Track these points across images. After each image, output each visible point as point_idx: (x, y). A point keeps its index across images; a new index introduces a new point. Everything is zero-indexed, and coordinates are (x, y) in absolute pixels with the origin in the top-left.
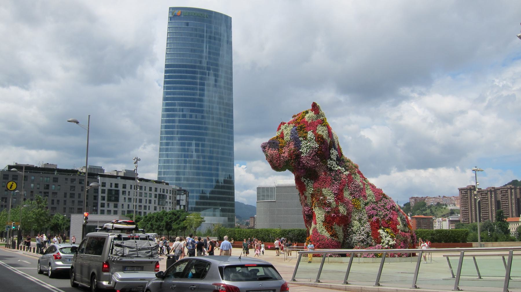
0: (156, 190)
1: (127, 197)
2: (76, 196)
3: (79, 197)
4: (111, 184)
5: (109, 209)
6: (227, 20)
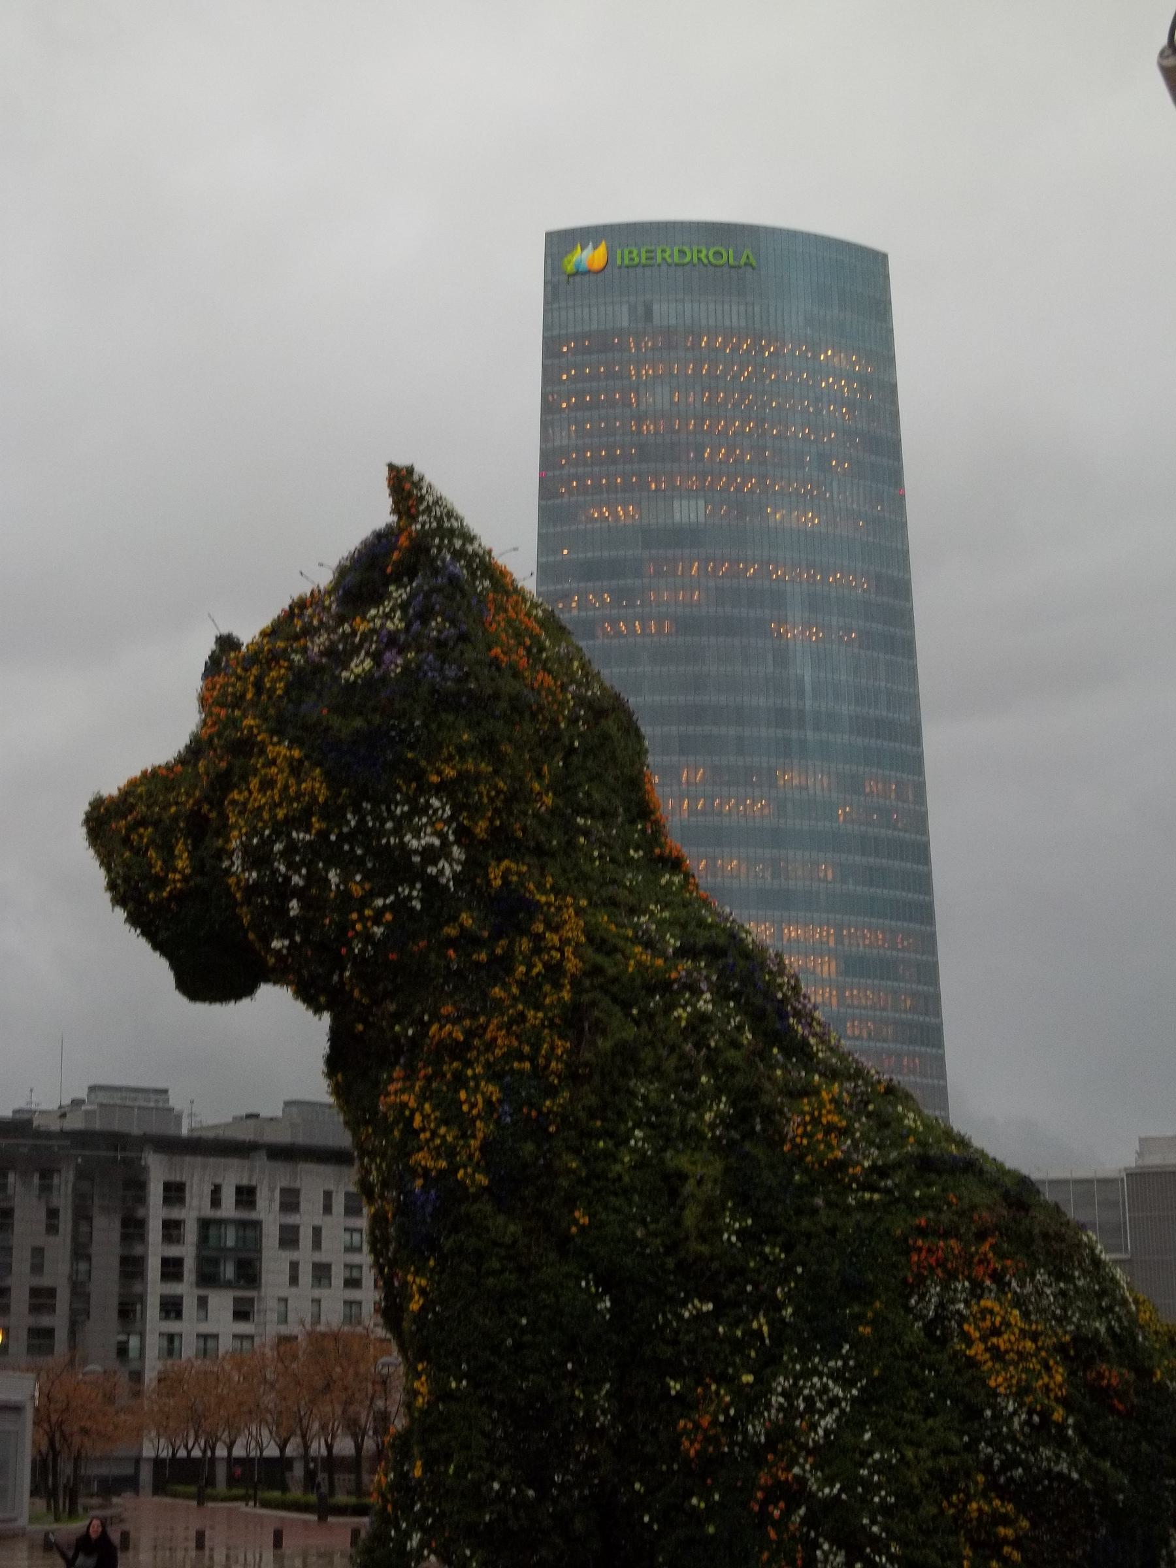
1: (305, 1255)
3: (37, 1268)
4: (216, 1190)
5: (205, 1328)
6: (854, 283)
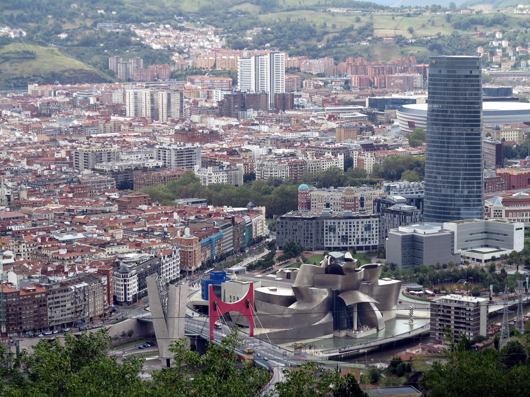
0: (362, 222)
1: (341, 228)
2: (309, 231)
